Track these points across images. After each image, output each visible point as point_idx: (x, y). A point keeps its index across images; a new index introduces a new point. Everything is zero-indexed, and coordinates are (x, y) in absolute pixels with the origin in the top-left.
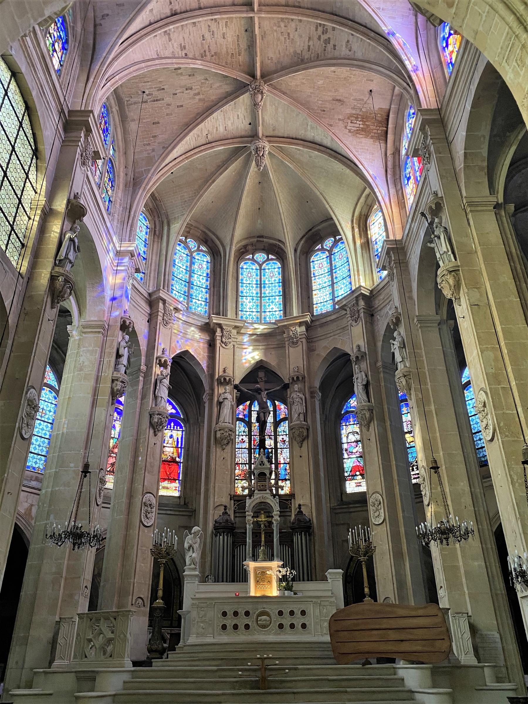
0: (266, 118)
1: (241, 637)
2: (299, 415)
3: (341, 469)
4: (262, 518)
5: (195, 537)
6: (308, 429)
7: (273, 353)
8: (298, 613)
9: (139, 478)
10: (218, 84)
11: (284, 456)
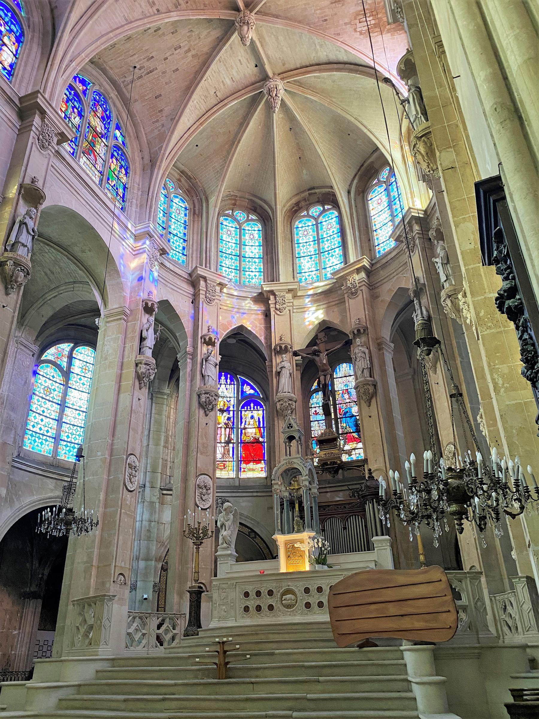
0: (270, 53)
1: (266, 619)
2: (363, 372)
5: (227, 514)
7: (336, 310)
9: (192, 462)
10: (205, 33)
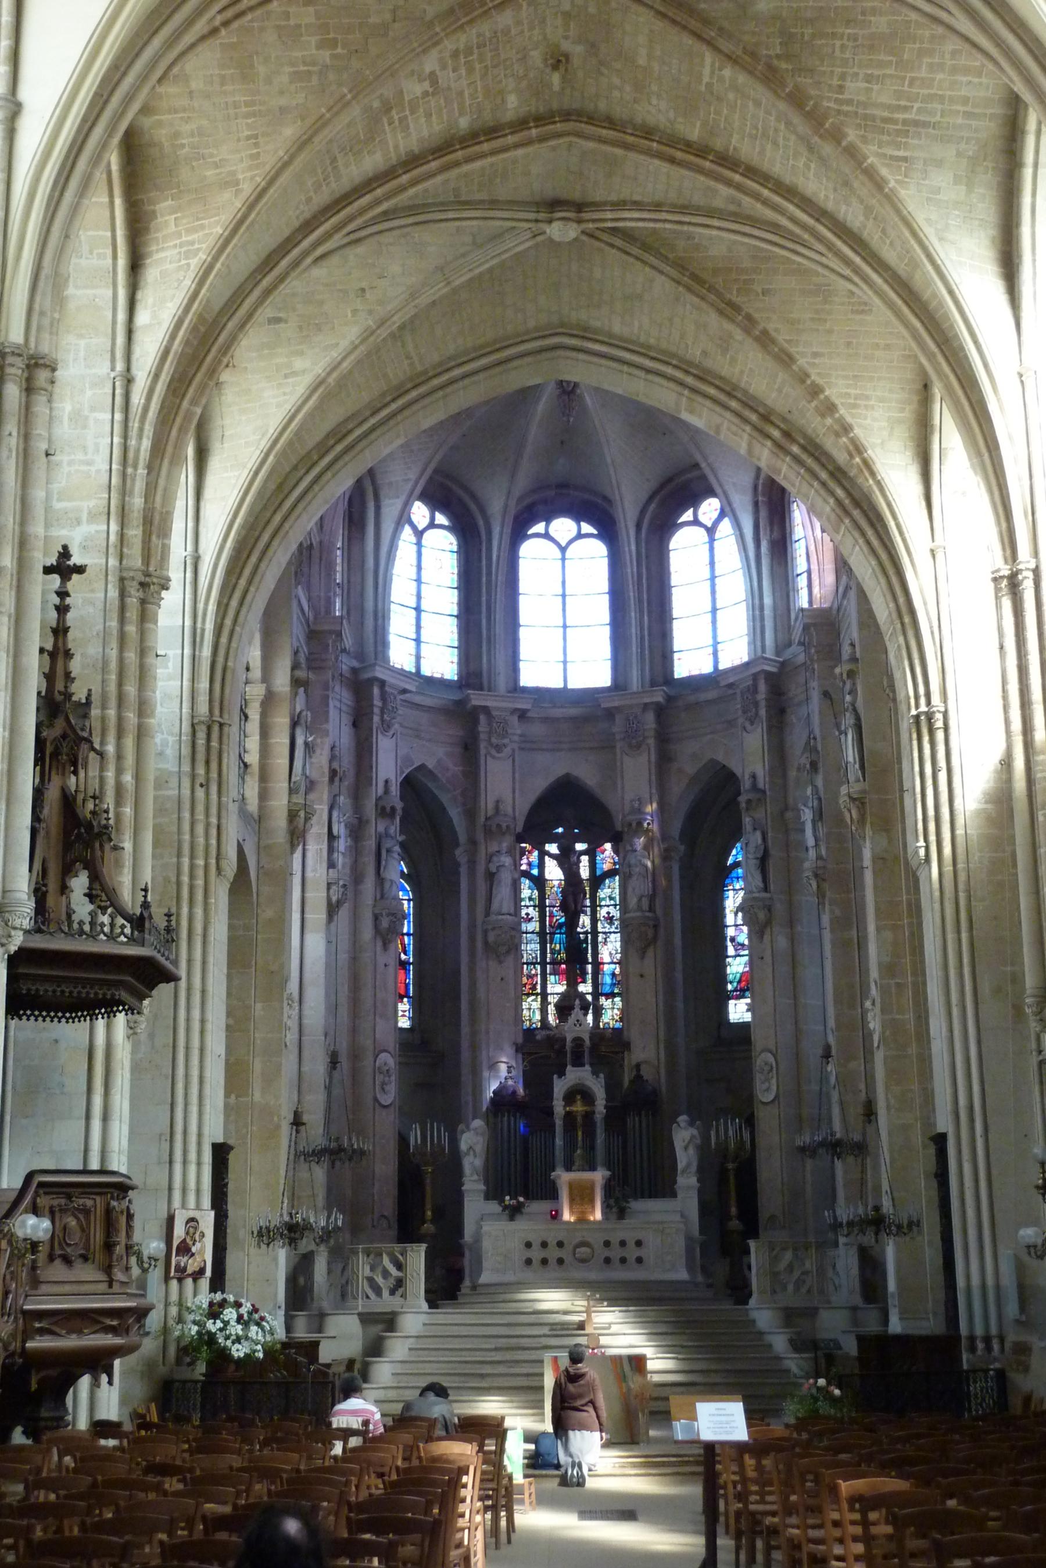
2: (640, 900)
3: (721, 976)
4: (579, 1107)
6: (656, 927)
8: (631, 1244)
11: (610, 949)
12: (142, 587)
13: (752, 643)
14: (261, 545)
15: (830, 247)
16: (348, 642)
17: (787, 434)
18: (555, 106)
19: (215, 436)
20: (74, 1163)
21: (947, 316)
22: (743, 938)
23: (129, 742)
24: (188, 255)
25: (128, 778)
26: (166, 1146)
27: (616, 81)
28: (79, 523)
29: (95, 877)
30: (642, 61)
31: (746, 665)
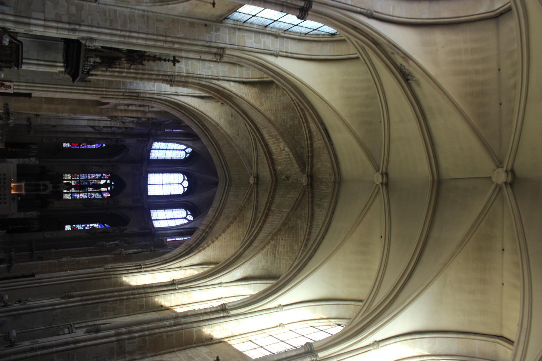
3: (76, 224)
12: (171, 80)
13: (159, 228)
14: (181, 110)
15: (248, 239)
16: (159, 132)
17: (207, 232)
18: (278, 177)
19: (206, 101)
20: (25, 55)
21: (234, 266)
22: (86, 228)
23: (133, 75)
24: (246, 94)
25: (124, 74)
26: (31, 81)
27: (284, 190)
28: (186, 66)
29: (99, 63)
30: (288, 196)
31: (153, 226)
